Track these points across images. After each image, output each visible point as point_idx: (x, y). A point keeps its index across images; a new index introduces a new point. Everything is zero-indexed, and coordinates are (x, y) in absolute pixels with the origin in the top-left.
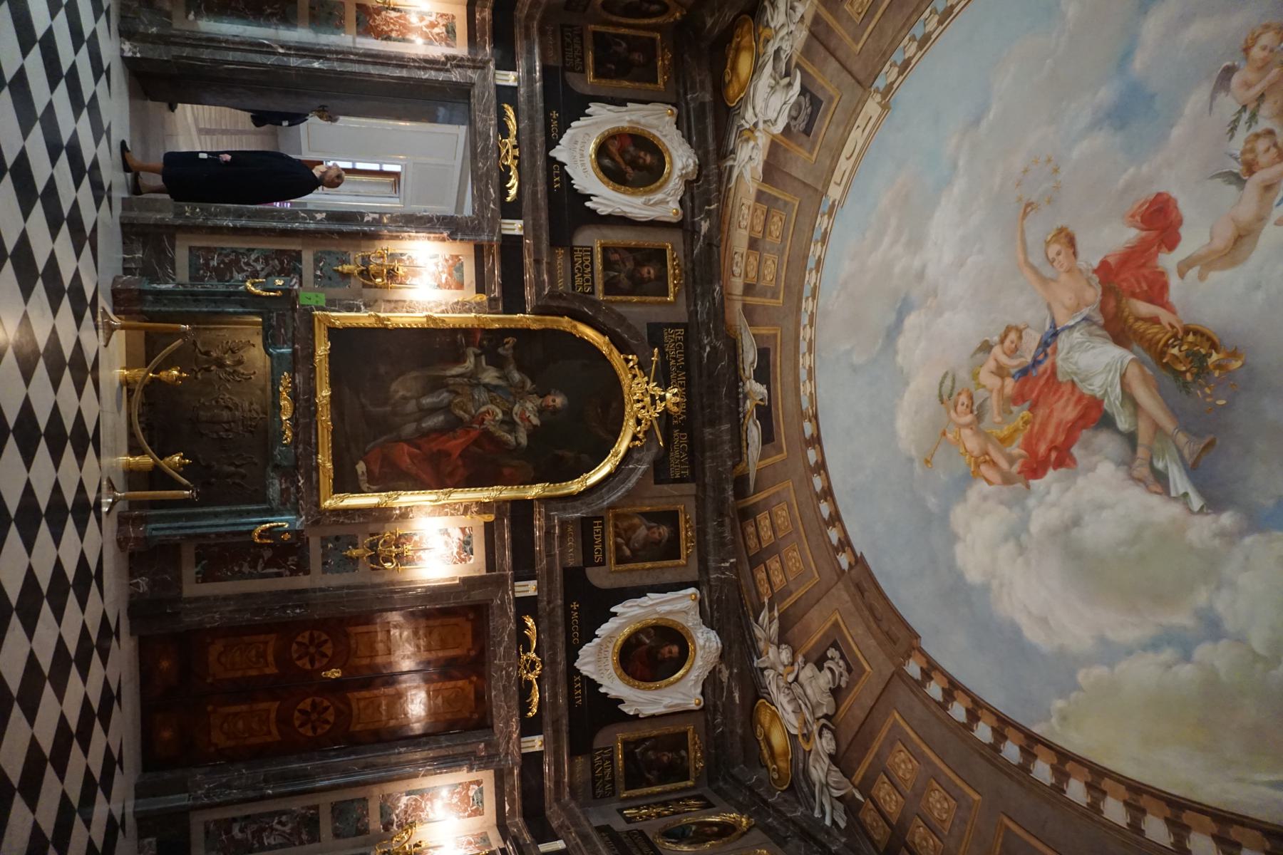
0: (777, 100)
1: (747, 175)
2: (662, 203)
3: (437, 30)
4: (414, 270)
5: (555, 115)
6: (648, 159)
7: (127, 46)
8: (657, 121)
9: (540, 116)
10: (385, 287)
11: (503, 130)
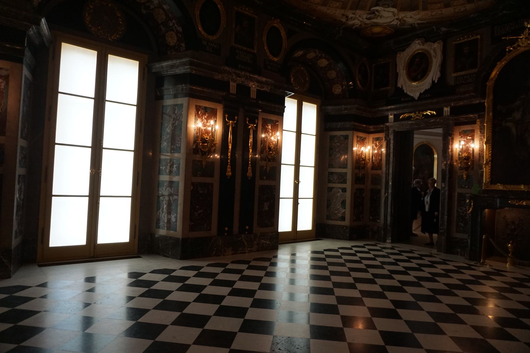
0: (385, 14)
1: (418, 17)
2: (435, 50)
3: (378, 144)
4: (467, 150)
5: (403, 99)
6: (417, 60)
7: (388, 241)
8: (403, 59)
9: (402, 105)
10: (473, 161)
11: (409, 118)
